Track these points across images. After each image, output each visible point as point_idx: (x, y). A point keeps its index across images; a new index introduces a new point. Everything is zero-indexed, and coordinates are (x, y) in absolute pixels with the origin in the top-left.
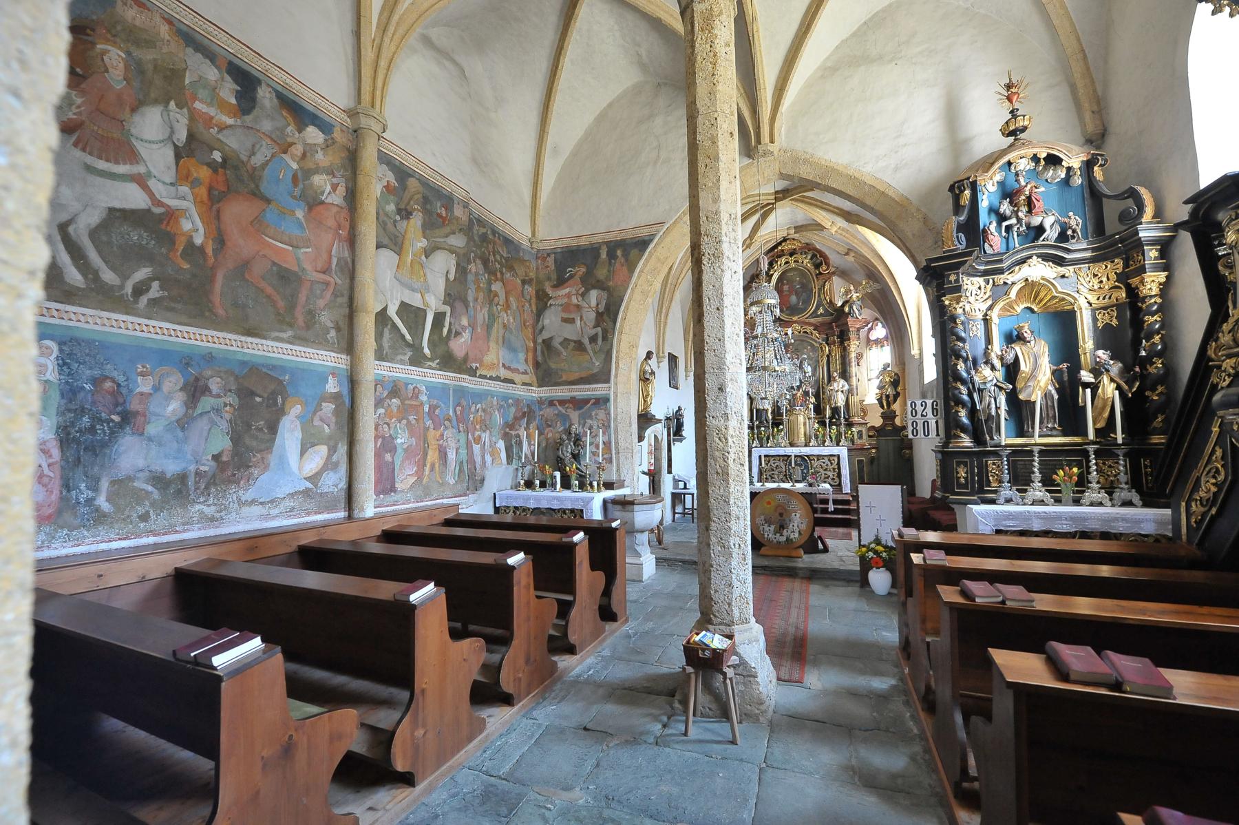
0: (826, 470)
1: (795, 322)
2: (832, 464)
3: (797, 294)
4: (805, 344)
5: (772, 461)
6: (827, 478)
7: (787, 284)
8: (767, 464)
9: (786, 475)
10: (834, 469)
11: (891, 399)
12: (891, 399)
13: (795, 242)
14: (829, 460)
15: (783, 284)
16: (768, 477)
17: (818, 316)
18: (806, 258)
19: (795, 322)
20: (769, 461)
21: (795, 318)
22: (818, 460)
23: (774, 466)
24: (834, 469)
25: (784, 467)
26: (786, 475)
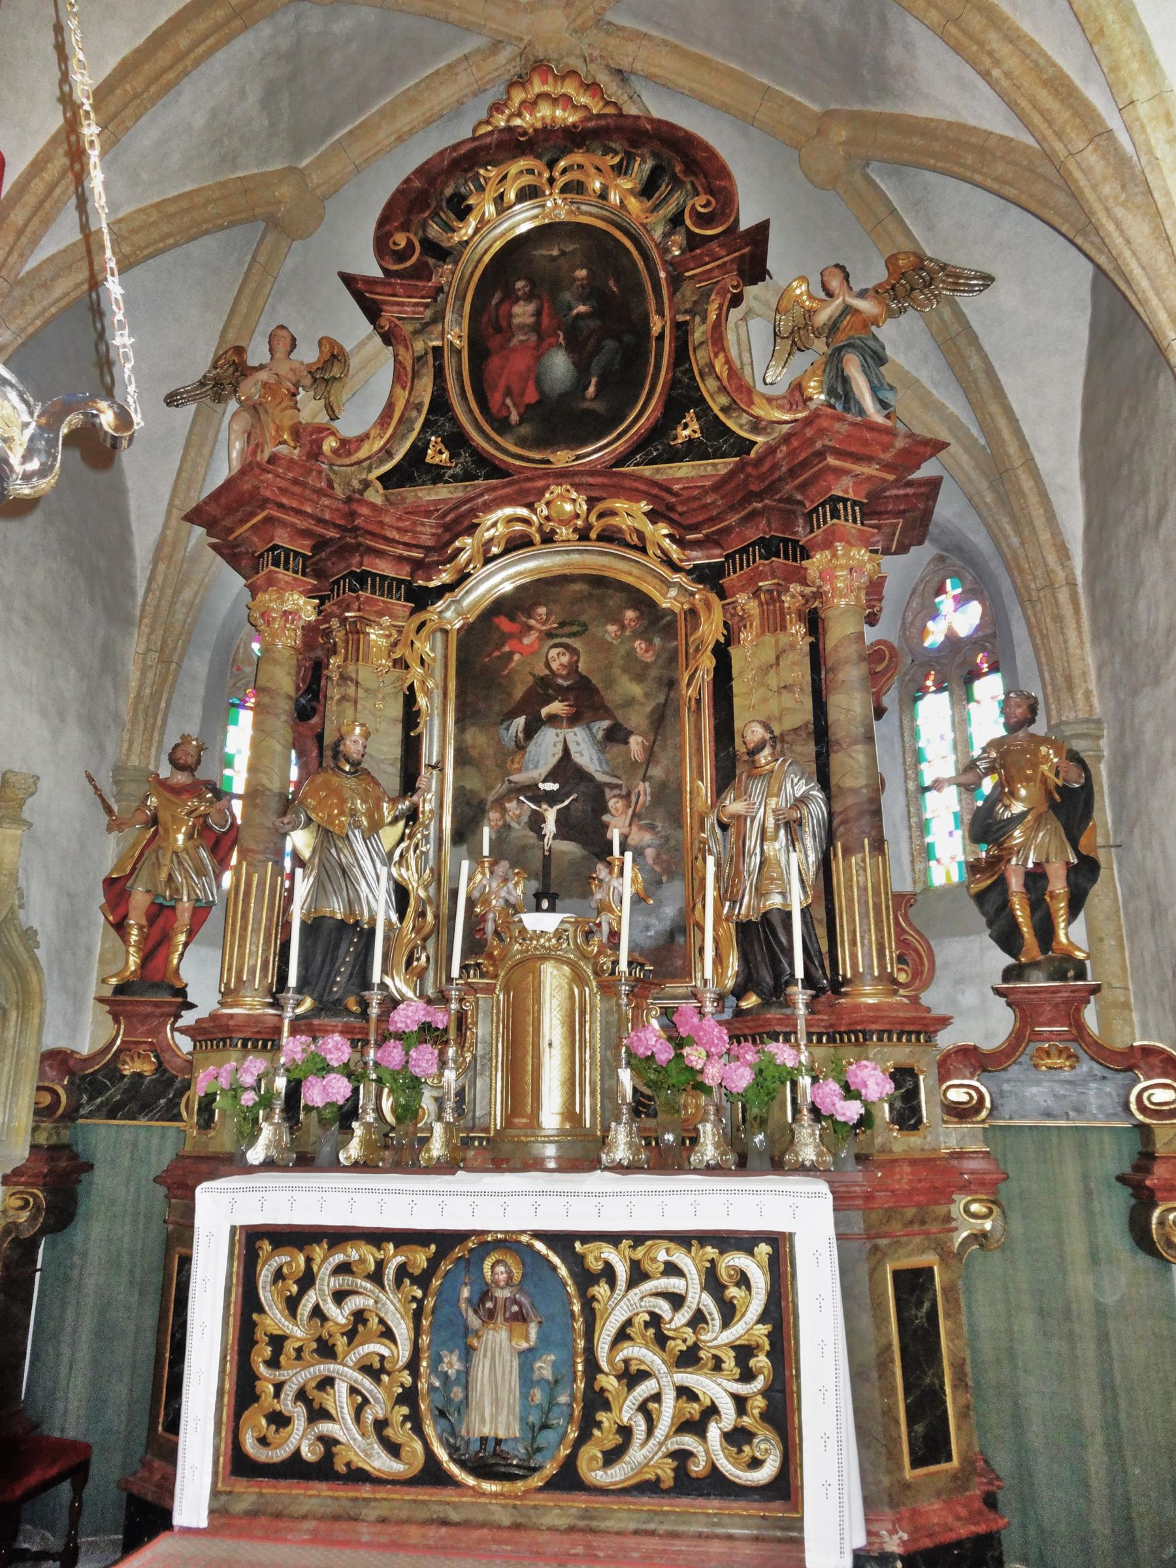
0: (689, 1359)
1: (562, 475)
2: (729, 1313)
3: (574, 346)
4: (615, 600)
5: (326, 1283)
6: (696, 1426)
7: (529, 298)
8: (292, 1305)
9: (409, 1397)
10: (744, 1353)
11: (1058, 885)
12: (1058, 885)
13: (569, 88)
14: (713, 1283)
15: (511, 297)
16: (288, 1404)
17: (674, 456)
18: (621, 170)
19: (562, 475)
20: (307, 1281)
21: (562, 458)
22: (638, 1275)
23: (339, 1316)
24: (744, 1353)
25: (402, 1330)
26: (409, 1397)
